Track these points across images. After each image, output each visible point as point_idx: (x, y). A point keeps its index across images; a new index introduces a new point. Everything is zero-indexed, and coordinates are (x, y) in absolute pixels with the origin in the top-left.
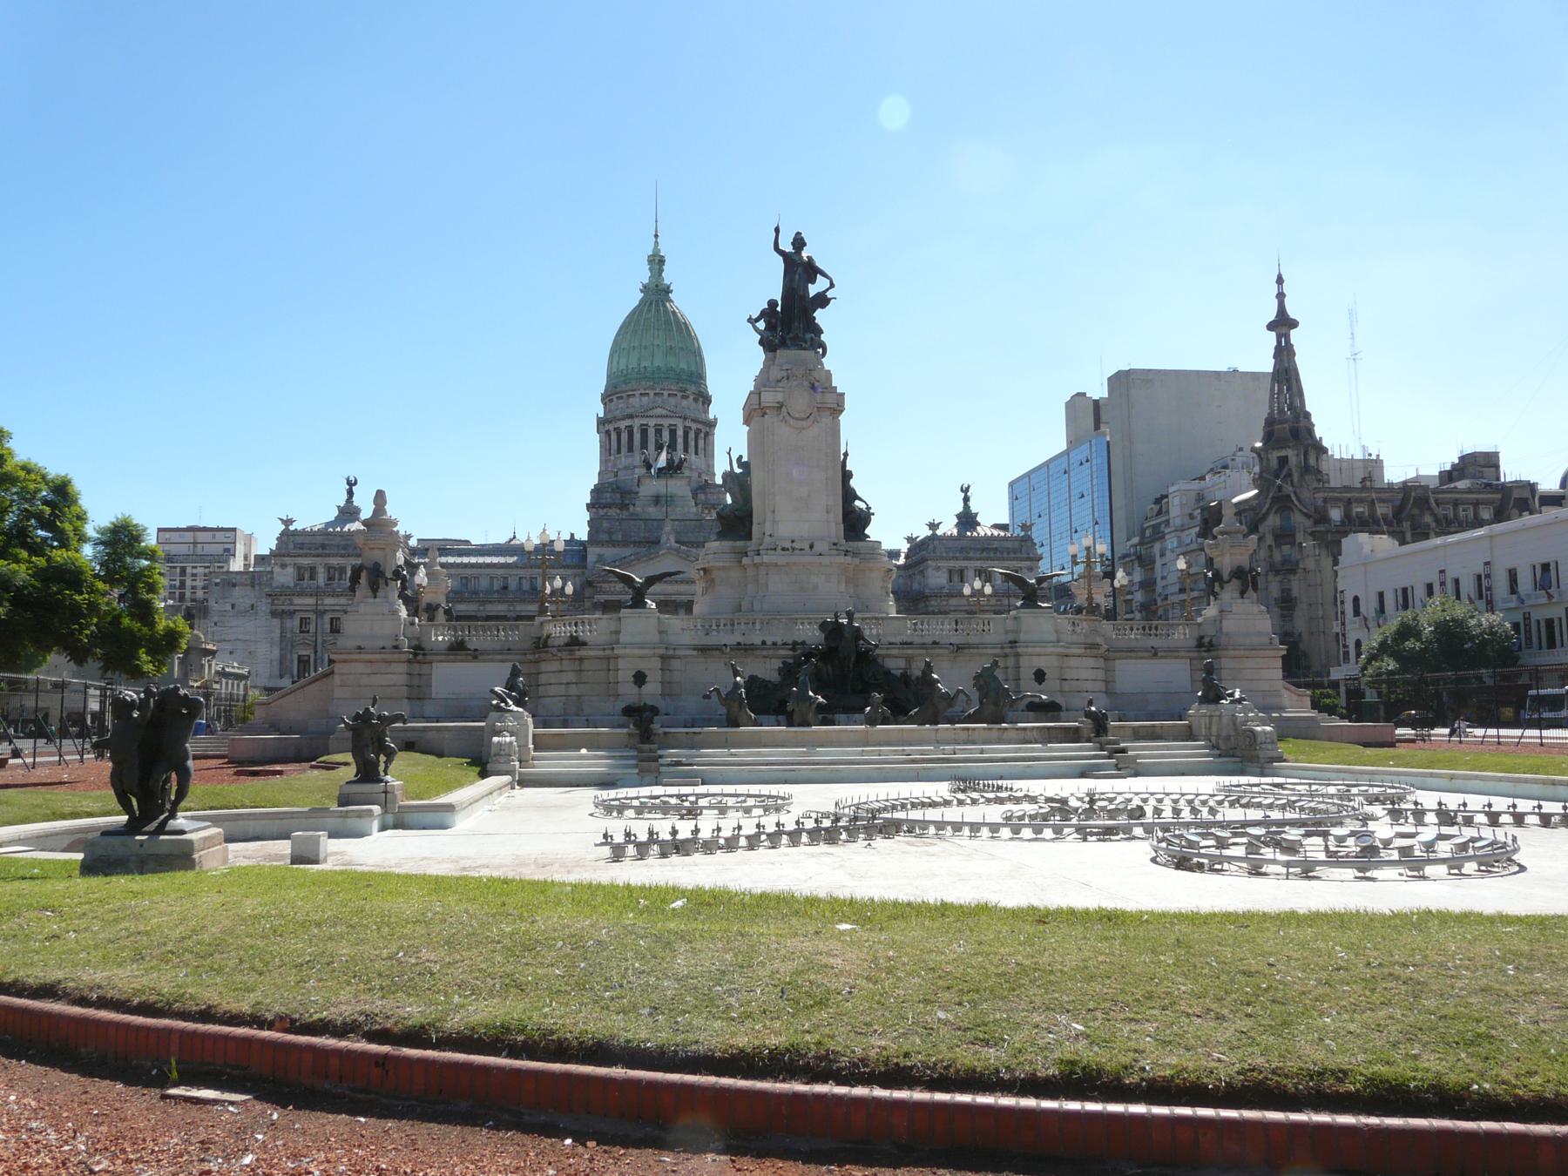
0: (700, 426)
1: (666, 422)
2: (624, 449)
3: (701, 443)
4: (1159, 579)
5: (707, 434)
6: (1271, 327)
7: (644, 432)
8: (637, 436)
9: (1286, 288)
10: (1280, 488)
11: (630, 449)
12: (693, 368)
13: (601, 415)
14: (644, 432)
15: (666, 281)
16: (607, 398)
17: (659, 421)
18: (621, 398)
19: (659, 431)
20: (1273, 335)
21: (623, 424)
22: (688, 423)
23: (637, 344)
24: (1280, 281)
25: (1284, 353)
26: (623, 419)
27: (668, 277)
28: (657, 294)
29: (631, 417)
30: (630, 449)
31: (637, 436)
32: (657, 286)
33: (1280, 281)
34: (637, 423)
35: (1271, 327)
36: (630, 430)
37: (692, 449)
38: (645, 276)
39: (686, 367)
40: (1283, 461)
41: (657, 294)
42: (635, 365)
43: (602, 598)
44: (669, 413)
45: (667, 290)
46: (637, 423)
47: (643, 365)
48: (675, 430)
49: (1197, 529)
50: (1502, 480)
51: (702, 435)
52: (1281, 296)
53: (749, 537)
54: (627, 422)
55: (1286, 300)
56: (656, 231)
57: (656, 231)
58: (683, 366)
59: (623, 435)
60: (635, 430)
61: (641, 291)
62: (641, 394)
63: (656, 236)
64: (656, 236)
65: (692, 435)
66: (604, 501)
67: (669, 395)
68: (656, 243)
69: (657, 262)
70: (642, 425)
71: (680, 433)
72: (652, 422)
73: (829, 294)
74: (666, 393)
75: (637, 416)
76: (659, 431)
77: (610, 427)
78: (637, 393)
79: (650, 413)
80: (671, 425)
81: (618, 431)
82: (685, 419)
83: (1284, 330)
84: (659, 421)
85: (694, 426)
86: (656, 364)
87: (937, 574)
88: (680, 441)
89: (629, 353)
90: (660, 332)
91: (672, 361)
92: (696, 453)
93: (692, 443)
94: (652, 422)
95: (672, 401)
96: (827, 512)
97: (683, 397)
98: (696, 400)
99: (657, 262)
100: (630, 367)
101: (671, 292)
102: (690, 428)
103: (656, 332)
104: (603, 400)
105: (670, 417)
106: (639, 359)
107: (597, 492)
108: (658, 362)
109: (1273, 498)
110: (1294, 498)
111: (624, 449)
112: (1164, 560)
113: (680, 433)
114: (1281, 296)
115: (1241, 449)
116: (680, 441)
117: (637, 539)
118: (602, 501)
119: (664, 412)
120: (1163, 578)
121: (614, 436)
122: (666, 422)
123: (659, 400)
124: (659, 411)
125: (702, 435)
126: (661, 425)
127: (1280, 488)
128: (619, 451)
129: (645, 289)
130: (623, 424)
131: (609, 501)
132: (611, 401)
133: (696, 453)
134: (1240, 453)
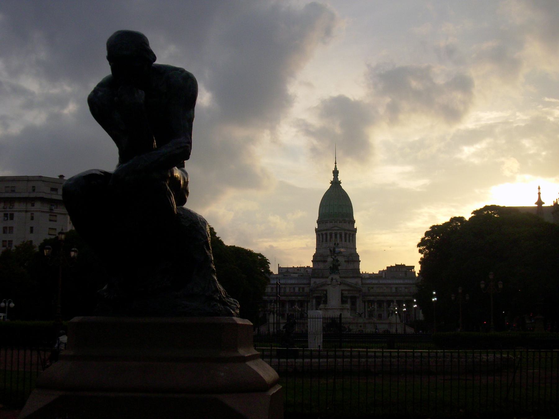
0: (350, 232)
1: (339, 232)
3: (351, 238)
7: (331, 234)
8: (329, 237)
9: (541, 191)
11: (326, 241)
13: (317, 228)
14: (331, 234)
15: (339, 180)
16: (318, 222)
17: (336, 231)
18: (323, 223)
21: (324, 232)
22: (346, 232)
24: (539, 188)
26: (324, 230)
27: (340, 178)
28: (336, 184)
29: (327, 230)
30: (326, 241)
31: (329, 237)
32: (336, 182)
33: (539, 188)
34: (328, 232)
36: (326, 234)
37: (348, 241)
38: (332, 178)
41: (336, 184)
43: (316, 295)
45: (340, 182)
46: (328, 232)
52: (539, 194)
53: (327, 304)
55: (541, 195)
56: (336, 161)
57: (336, 161)
59: (324, 236)
60: (328, 234)
61: (330, 183)
62: (330, 222)
63: (336, 163)
64: (336, 163)
65: (348, 236)
67: (340, 222)
68: (336, 166)
69: (336, 173)
70: (330, 233)
71: (343, 235)
72: (333, 232)
74: (338, 221)
75: (329, 230)
77: (320, 233)
78: (329, 221)
79: (333, 229)
81: (322, 235)
85: (348, 232)
88: (343, 238)
92: (349, 242)
93: (348, 239)
94: (333, 232)
97: (344, 222)
99: (336, 173)
101: (341, 183)
102: (347, 233)
104: (317, 223)
105: (340, 230)
107: (315, 256)
111: (324, 241)
113: (343, 235)
114: (539, 194)
116: (343, 238)
121: (321, 236)
122: (339, 232)
125: (351, 235)
128: (322, 242)
129: (332, 183)
130: (324, 232)
132: (320, 223)
133: (349, 242)
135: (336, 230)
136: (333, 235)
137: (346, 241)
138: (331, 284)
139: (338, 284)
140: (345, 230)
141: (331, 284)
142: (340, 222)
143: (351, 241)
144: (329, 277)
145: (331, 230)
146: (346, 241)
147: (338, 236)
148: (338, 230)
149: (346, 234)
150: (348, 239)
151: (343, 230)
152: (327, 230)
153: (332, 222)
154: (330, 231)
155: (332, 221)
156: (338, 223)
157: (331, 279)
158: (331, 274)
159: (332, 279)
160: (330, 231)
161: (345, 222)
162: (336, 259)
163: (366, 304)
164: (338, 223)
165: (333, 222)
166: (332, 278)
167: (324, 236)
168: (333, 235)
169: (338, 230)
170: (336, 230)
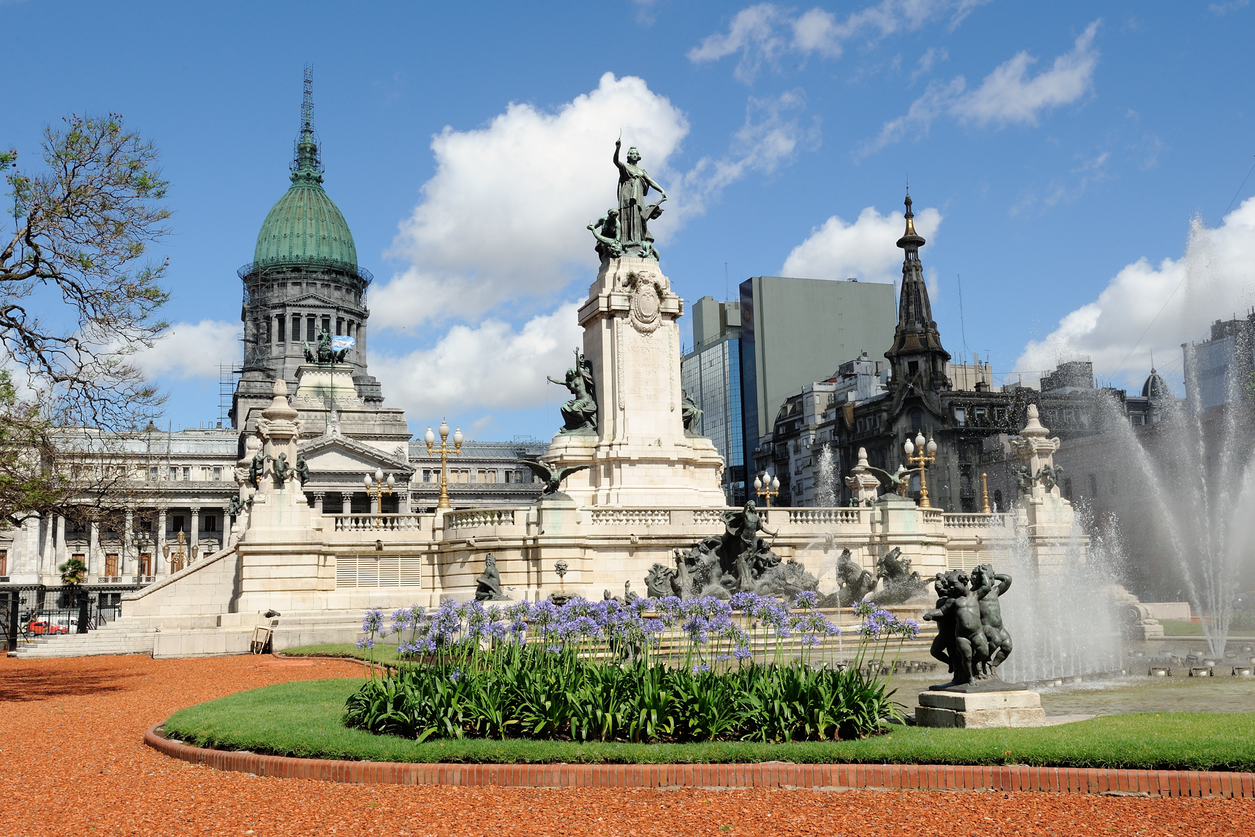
0: (353, 317)
1: (319, 312)
2: (275, 337)
4: (793, 474)
5: (359, 326)
6: (901, 243)
7: (296, 319)
8: (289, 325)
10: (912, 390)
11: (282, 337)
14: (296, 319)
17: (312, 311)
19: (311, 321)
20: (902, 250)
22: (341, 314)
23: (288, 232)
25: (911, 267)
31: (289, 325)
34: (289, 311)
35: (901, 243)
39: (339, 259)
40: (914, 366)
44: (322, 304)
48: (328, 321)
49: (833, 427)
50: (1095, 387)
51: (355, 326)
54: (279, 311)
58: (336, 256)
66: (254, 391)
70: (294, 314)
75: (289, 305)
76: (311, 321)
80: (324, 315)
82: (338, 309)
83: (912, 248)
84: (312, 311)
85: (347, 317)
89: (279, 240)
90: (313, 221)
91: (325, 252)
94: (304, 312)
95: (326, 291)
98: (348, 291)
102: (343, 319)
103: (309, 221)
105: (324, 307)
106: (290, 247)
109: (905, 399)
110: (923, 398)
111: (275, 337)
112: (797, 457)
115: (865, 354)
118: (251, 390)
120: (797, 473)
123: (312, 291)
124: (311, 302)
126: (314, 315)
127: (912, 390)
131: (258, 391)
134: (865, 359)
135: (312, 306)
136: (304, 323)
145: (294, 306)
148: (320, 307)
151: (332, 308)
152: (283, 306)
153: (300, 284)
154: (296, 310)
156: (319, 286)
160: (296, 310)
164: (319, 286)
165: (304, 285)
168: (304, 323)
169: (320, 307)
170: (309, 306)
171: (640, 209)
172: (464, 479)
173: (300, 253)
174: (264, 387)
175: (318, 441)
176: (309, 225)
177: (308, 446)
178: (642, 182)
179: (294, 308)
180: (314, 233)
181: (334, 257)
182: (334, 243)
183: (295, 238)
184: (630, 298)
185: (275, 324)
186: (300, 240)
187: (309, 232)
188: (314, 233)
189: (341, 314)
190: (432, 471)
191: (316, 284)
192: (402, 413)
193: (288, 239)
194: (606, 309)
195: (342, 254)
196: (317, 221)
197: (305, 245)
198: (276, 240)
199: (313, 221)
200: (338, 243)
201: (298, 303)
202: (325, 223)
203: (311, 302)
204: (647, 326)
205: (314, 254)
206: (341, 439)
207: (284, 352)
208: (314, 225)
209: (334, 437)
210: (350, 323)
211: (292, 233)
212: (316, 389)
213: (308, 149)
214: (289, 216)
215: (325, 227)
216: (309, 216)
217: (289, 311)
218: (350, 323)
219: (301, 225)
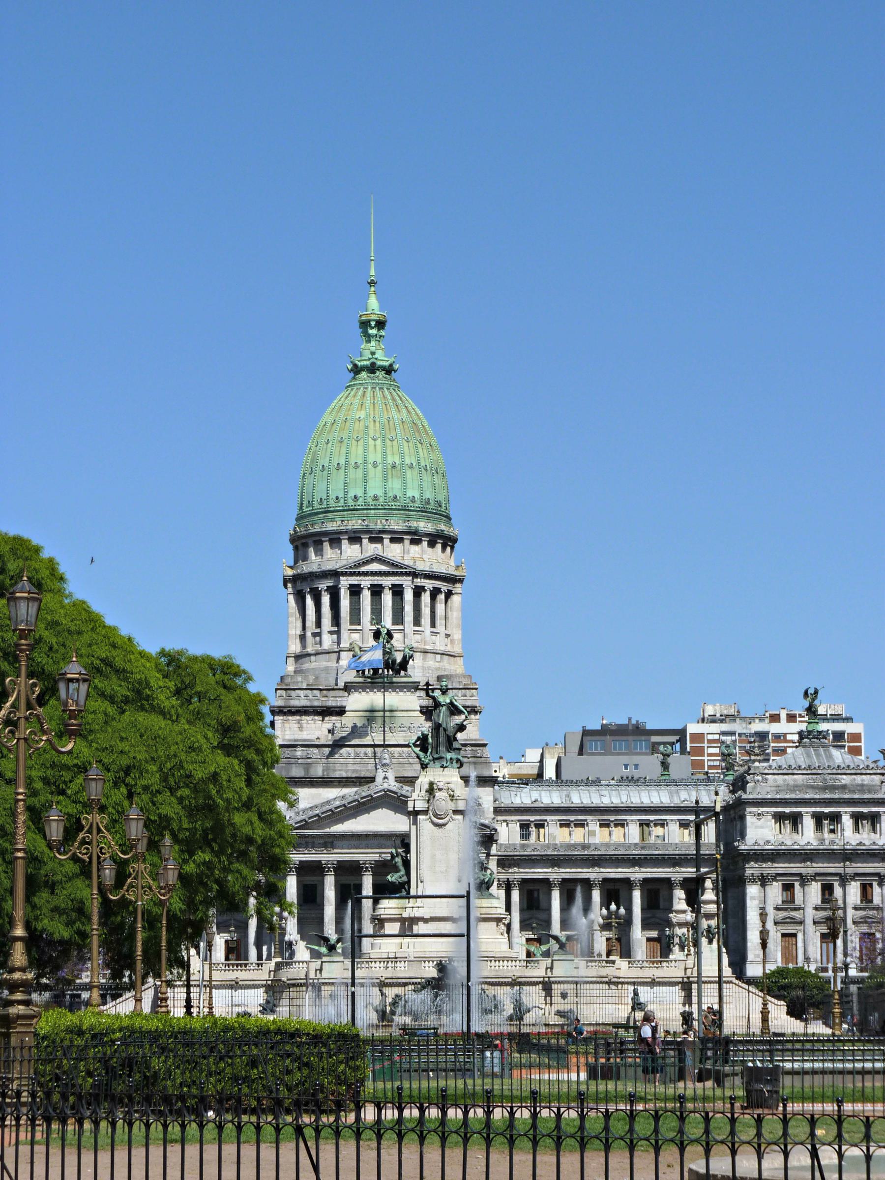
0: (438, 584)
1: (388, 582)
3: (440, 607)
5: (449, 594)
12: (428, 495)
17: (377, 580)
21: (323, 585)
22: (419, 582)
23: (342, 462)
39: (417, 496)
42: (341, 495)
47: (351, 494)
51: (442, 597)
54: (329, 583)
58: (413, 492)
60: (342, 591)
65: (426, 598)
71: (409, 595)
73: (465, 723)
75: (345, 574)
79: (363, 569)
84: (377, 580)
85: (429, 584)
86: (371, 493)
87: (760, 823)
88: (409, 608)
91: (395, 487)
93: (426, 611)
94: (366, 582)
96: (459, 881)
98: (432, 544)
100: (333, 496)
103: (371, 442)
108: (375, 488)
113: (409, 595)
116: (409, 608)
117: (344, 775)
119: (384, 568)
125: (442, 597)
137: (417, 622)
138: (425, 812)
139: (456, 812)
140: (414, 574)
141: (425, 812)
142: (393, 540)
143: (439, 622)
144: (418, 777)
146: (417, 622)
147: (387, 598)
149: (418, 592)
150: (426, 611)
151: (407, 574)
154: (354, 580)
155: (358, 535)
156: (386, 542)
157: (426, 786)
158: (424, 766)
159: (431, 790)
160: (354, 580)
161: (415, 542)
162: (448, 701)
163: (515, 895)
164: (386, 542)
166: (431, 784)
167: (326, 599)
168: (366, 596)
171: (445, 730)
172: (578, 836)
173: (360, 493)
174: (311, 697)
175: (365, 791)
176: (371, 448)
177: (350, 799)
178: (449, 708)
179: (350, 578)
180: (379, 461)
181: (410, 494)
182: (409, 473)
183: (351, 471)
184: (428, 801)
185: (326, 599)
186: (360, 473)
187: (371, 459)
188: (379, 461)
189: (419, 582)
190: (532, 825)
191: (382, 538)
192: (484, 745)
193: (342, 471)
194: (412, 809)
195: (421, 488)
196: (384, 441)
197: (365, 480)
198: (325, 472)
199: (379, 442)
200: (416, 472)
201: (357, 570)
202: (395, 443)
203: (375, 567)
204: (440, 821)
205: (380, 493)
206: (394, 789)
207: (339, 643)
208: (379, 448)
209: (386, 786)
210: (435, 593)
211: (347, 462)
212: (367, 714)
213: (373, 323)
214: (345, 435)
215: (396, 449)
216: (371, 434)
217: (345, 582)
218: (435, 593)
219: (360, 450)
